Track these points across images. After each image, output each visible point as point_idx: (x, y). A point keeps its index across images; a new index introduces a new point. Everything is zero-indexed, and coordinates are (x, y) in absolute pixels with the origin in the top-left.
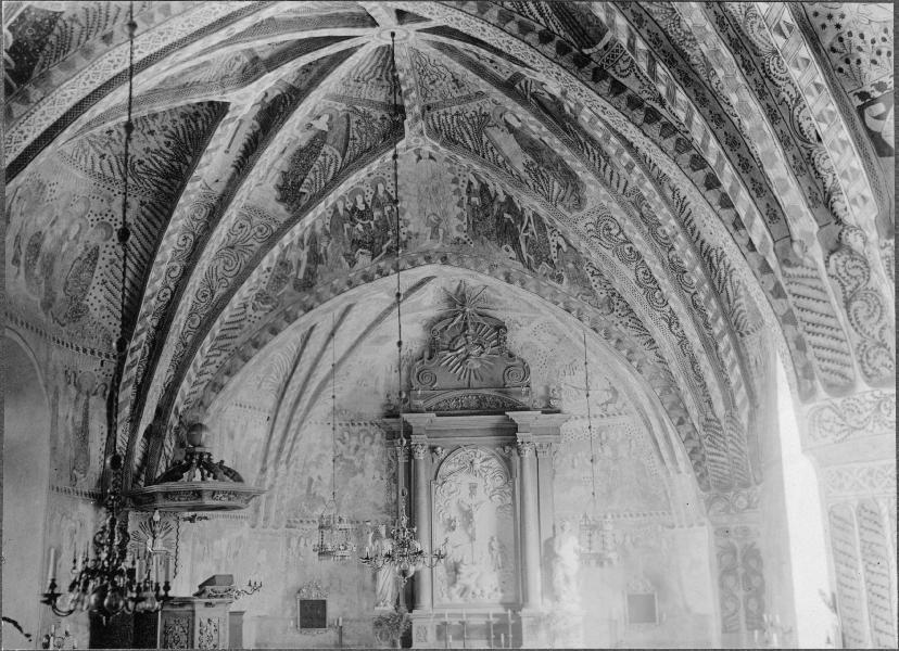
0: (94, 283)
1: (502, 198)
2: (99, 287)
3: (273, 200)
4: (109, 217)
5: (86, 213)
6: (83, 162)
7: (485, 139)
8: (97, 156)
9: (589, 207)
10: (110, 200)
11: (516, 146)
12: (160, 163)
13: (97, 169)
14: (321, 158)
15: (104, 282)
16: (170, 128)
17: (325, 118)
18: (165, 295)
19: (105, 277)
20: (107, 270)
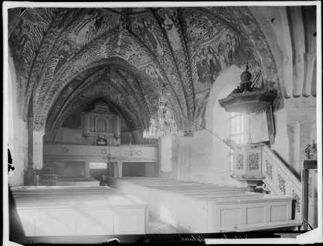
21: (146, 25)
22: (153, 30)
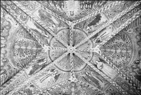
1: (57, 5)
3: (102, 17)
6: (131, 45)
7: (59, 22)
8: (128, 44)
9: (37, 11)
11: (54, 21)
12: (118, 37)
13: (130, 41)
14: (90, 22)
17: (87, 29)
18: (135, 10)
21: (87, 74)
22: (92, 74)
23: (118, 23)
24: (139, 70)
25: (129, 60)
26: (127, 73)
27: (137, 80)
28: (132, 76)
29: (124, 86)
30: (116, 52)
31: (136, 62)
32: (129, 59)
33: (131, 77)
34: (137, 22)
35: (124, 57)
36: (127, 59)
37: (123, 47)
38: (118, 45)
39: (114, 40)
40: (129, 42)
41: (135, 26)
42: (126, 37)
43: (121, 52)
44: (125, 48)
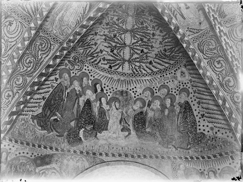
0: (197, 119)
2: (201, 120)
4: (182, 85)
5: (169, 91)
8: (148, 65)
10: (176, 78)
13: (155, 70)
15: (203, 116)
16: (154, 25)
19: (201, 113)
20: (200, 109)
23: (211, 47)
24: (78, 93)
25: (103, 66)
26: (66, 65)
27: (51, 90)
28: (61, 77)
29: (28, 61)
30: (126, 31)
31: (98, 86)
32: (107, 67)
33: (57, 76)
34: (204, 97)
35: (112, 54)
36: (106, 62)
37: (139, 52)
38: (145, 40)
39: (161, 31)
40: (153, 68)
41: (195, 89)
42: (168, 63)
43: (125, 44)
44: (136, 56)
